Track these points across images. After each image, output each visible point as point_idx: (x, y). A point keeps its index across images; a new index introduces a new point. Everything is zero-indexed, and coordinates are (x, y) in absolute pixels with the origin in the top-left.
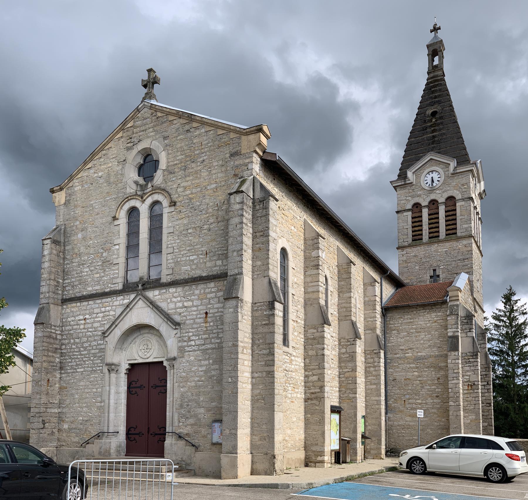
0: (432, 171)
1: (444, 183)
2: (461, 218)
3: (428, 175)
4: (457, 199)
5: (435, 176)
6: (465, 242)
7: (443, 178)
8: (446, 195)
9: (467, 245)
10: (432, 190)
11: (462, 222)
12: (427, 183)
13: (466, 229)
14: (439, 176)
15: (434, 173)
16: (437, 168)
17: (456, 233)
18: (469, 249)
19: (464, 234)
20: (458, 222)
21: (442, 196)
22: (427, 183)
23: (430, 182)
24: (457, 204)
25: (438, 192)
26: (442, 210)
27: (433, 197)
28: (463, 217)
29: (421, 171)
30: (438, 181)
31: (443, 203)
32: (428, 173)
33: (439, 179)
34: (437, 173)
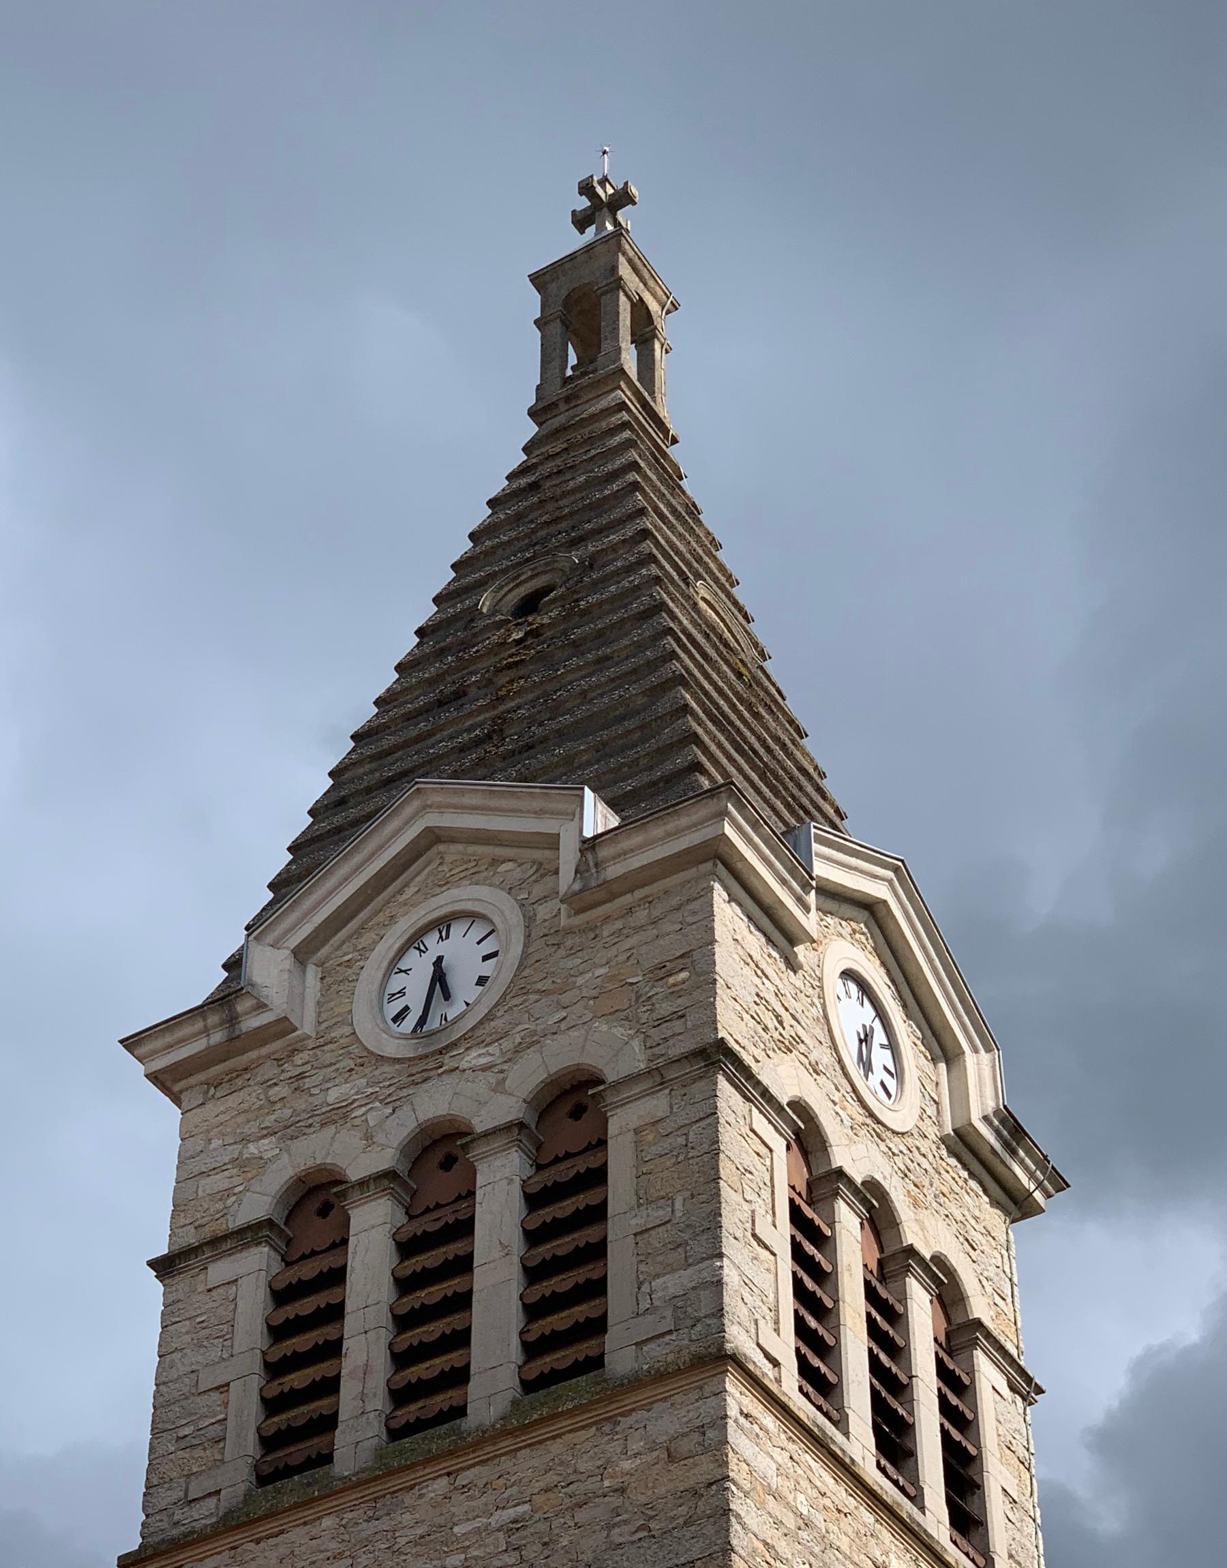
0: (442, 925)
1: (519, 988)
2: (636, 1223)
3: (411, 959)
4: (611, 1077)
5: (462, 951)
6: (666, 1420)
7: (517, 950)
8: (530, 1074)
9: (685, 1446)
10: (433, 1052)
11: (643, 1258)
12: (400, 1017)
13: (679, 1304)
14: (488, 947)
15: (457, 929)
16: (483, 892)
17: (596, 1362)
18: (704, 1469)
19: (658, 1353)
20: (620, 1264)
21: (499, 1087)
22: (400, 1017)
23: (415, 999)
24: (622, 1123)
25: (474, 1058)
26: (499, 1194)
27: (434, 1102)
28: (663, 1214)
29: (364, 941)
30: (482, 981)
31: (507, 1128)
32: (415, 941)
33: (488, 968)
34: (479, 931)
